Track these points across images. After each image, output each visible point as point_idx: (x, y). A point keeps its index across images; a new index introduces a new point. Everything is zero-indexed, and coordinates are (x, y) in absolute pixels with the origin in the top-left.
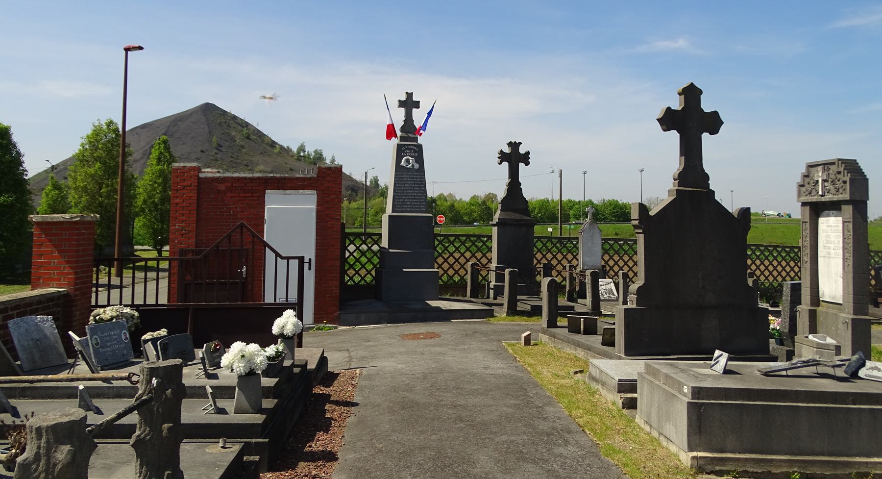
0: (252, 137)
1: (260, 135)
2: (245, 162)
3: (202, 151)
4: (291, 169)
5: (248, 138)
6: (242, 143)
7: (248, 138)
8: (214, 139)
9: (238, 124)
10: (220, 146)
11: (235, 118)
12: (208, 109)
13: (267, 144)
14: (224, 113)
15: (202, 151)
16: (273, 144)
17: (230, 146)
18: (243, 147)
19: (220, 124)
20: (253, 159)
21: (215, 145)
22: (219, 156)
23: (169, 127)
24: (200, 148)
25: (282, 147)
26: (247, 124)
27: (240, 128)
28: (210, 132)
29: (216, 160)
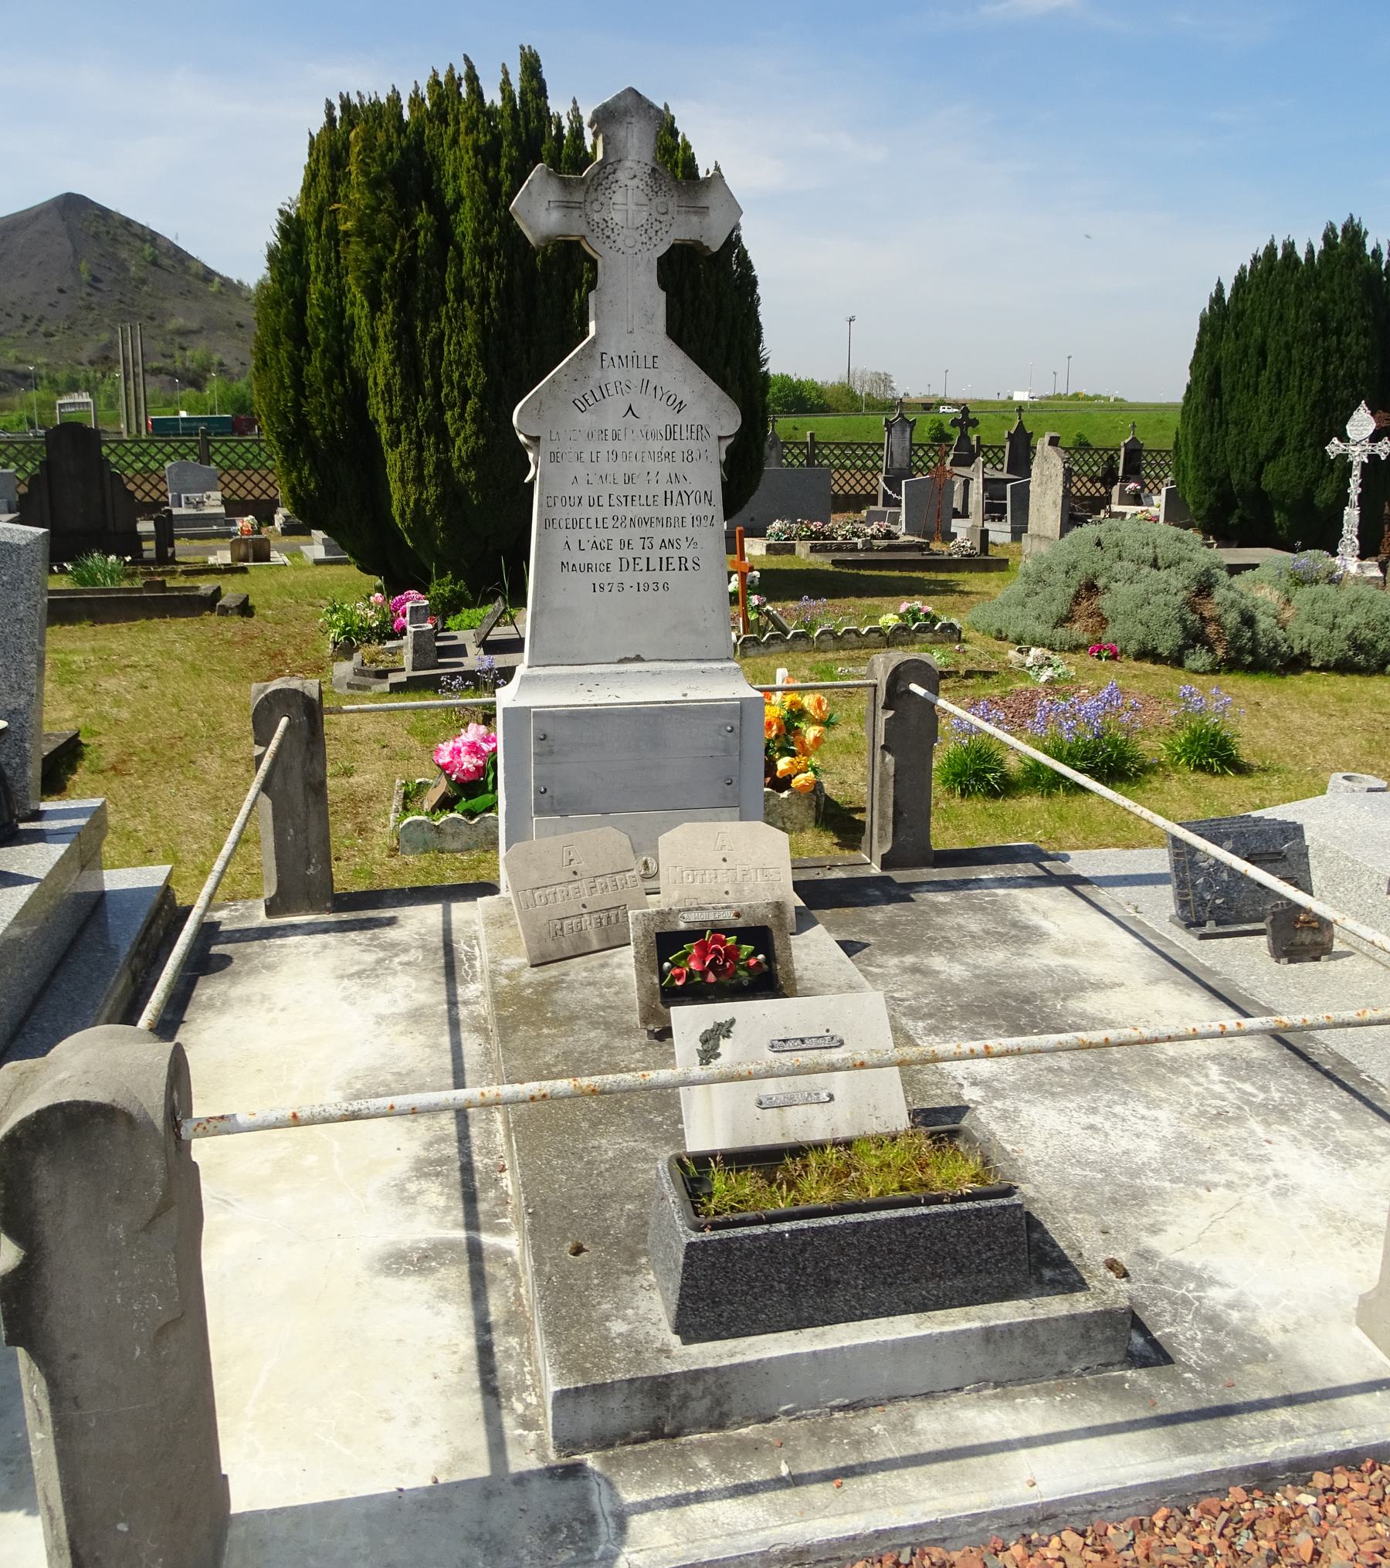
0: (166, 262)
1: (181, 257)
2: (147, 312)
3: (61, 291)
4: (240, 326)
5: (154, 263)
8: (83, 266)
9: (135, 235)
10: (96, 279)
11: (128, 223)
12: (72, 205)
13: (197, 276)
14: (105, 214)
15: (61, 291)
16: (208, 275)
17: (116, 281)
18: (144, 282)
19: (96, 236)
21: (85, 276)
22: (94, 299)
24: (56, 285)
25: (226, 282)
27: (138, 243)
28: (75, 251)
29: (89, 308)
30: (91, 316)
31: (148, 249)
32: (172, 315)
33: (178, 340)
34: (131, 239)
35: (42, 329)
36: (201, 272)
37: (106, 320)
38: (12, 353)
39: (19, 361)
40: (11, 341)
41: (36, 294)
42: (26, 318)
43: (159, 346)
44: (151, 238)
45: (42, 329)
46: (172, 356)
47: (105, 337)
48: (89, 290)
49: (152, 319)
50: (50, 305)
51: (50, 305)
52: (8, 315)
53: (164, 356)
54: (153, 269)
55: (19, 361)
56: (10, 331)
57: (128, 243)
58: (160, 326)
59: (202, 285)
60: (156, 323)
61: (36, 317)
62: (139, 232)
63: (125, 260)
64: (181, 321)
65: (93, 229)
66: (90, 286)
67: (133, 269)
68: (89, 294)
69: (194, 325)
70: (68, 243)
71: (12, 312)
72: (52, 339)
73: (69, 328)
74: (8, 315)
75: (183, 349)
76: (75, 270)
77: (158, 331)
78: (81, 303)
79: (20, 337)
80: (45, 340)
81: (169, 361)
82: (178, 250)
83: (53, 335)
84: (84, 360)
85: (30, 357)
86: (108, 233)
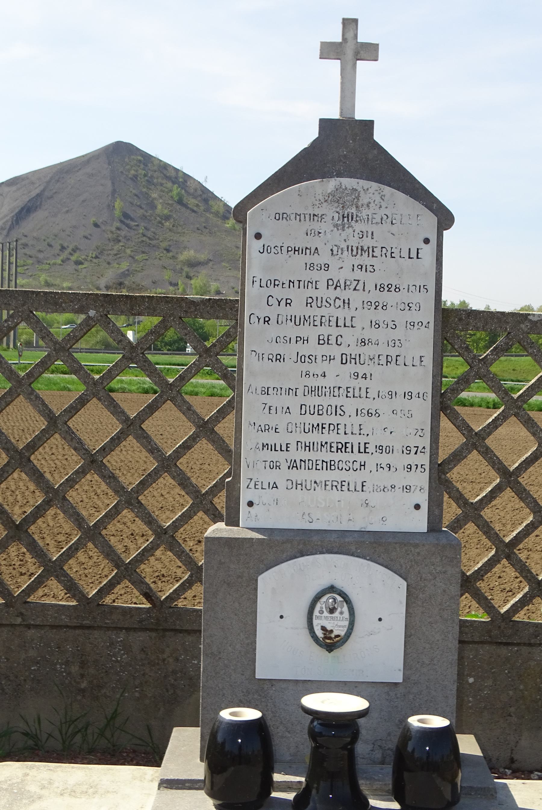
0: (192, 202)
2: (164, 245)
3: (96, 225)
5: (180, 202)
6: (166, 212)
7: (180, 202)
8: (118, 204)
9: (168, 178)
10: (126, 215)
11: (165, 167)
13: (216, 214)
14: (147, 159)
15: (96, 225)
17: (144, 218)
20: (182, 239)
21: (117, 213)
22: (123, 233)
23: (48, 182)
26: (187, 177)
27: (169, 185)
28: (114, 192)
30: (116, 247)
31: (176, 190)
32: (185, 248)
33: (186, 269)
34: (164, 181)
35: (73, 258)
36: (222, 210)
37: (128, 251)
38: (43, 277)
39: (48, 284)
40: (47, 267)
41: (75, 227)
42: (63, 248)
43: (167, 275)
44: (180, 179)
45: (73, 258)
46: (177, 285)
47: (125, 266)
48: (118, 224)
49: (168, 251)
50: (86, 237)
51: (86, 237)
52: (50, 245)
53: (171, 284)
54: (179, 207)
55: (48, 284)
56: (48, 258)
57: (162, 185)
58: (173, 257)
59: (220, 222)
60: (171, 254)
61: (71, 247)
62: (173, 174)
63: (155, 199)
64: (192, 252)
65: (133, 172)
66: (121, 222)
67: (159, 207)
68: (118, 229)
69: (202, 257)
70: (109, 184)
71: (53, 243)
72: (81, 267)
73: (96, 257)
74: (50, 245)
75: (189, 277)
76: (111, 208)
77: (171, 261)
78: (110, 236)
79: (55, 264)
80: (75, 267)
81: (171, 288)
82: (205, 190)
83: (81, 263)
84: (102, 286)
85: (58, 282)
86: (145, 175)
